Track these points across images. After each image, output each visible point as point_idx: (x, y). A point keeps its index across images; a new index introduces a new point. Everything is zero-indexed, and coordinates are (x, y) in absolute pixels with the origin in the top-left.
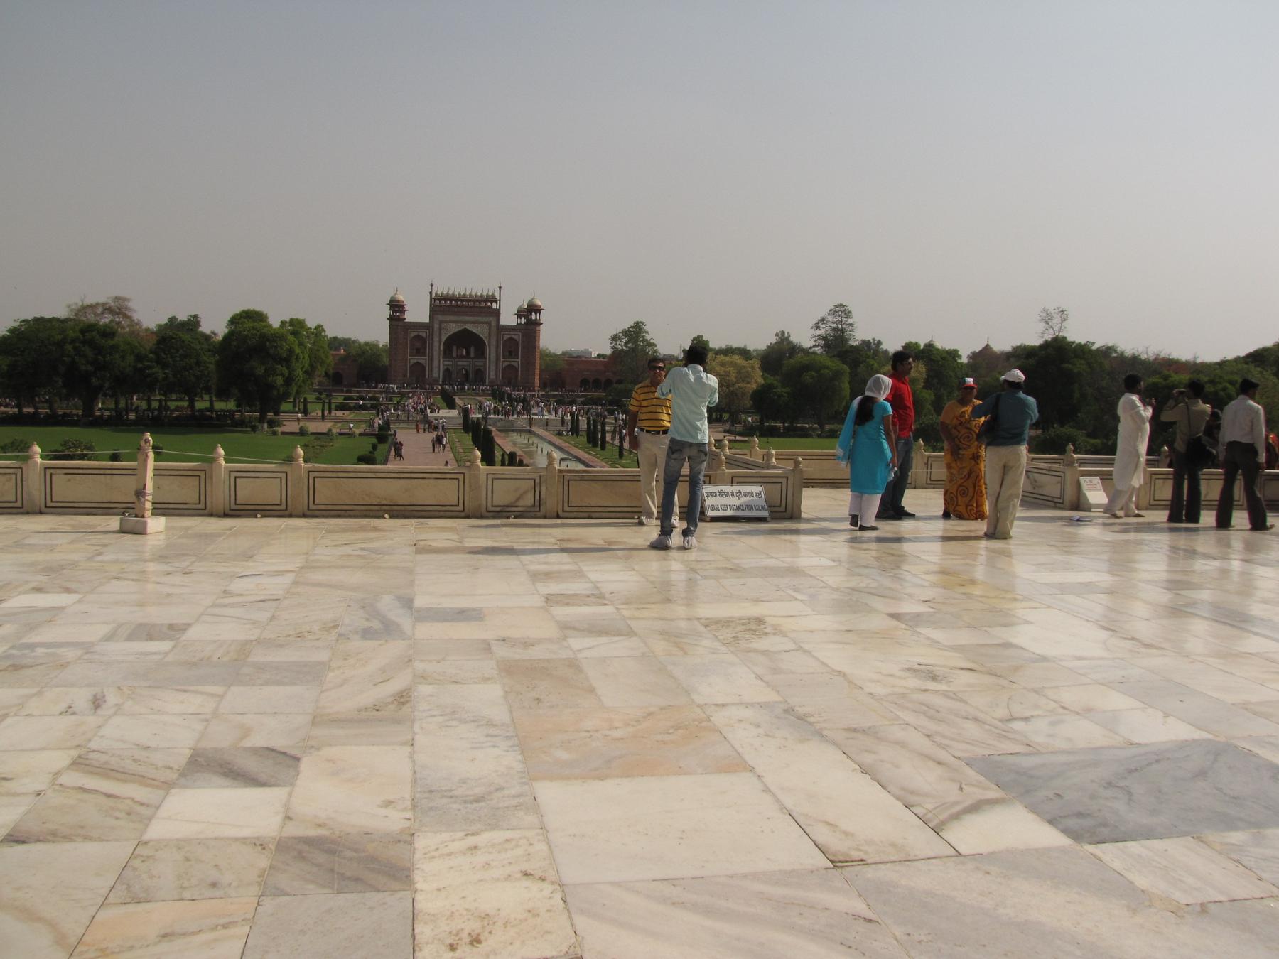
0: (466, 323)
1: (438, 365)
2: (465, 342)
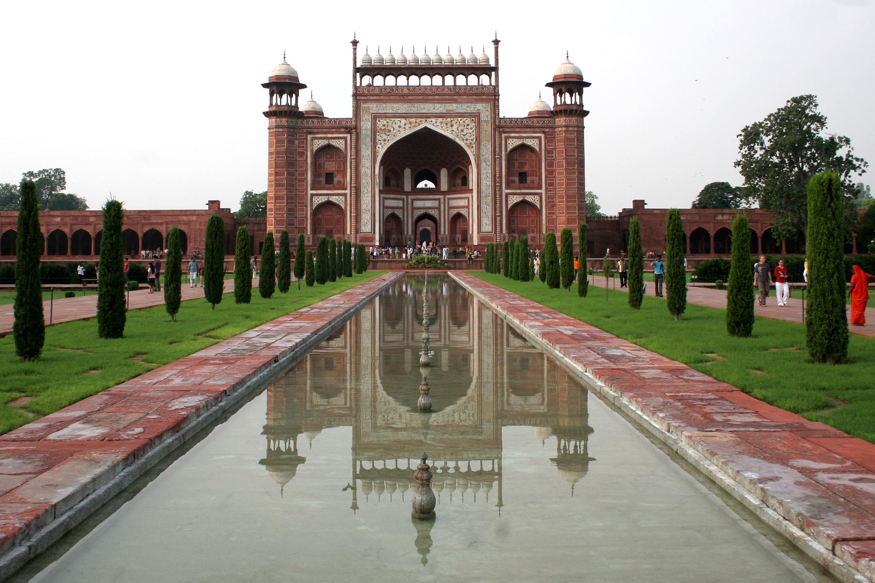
0: (427, 116)
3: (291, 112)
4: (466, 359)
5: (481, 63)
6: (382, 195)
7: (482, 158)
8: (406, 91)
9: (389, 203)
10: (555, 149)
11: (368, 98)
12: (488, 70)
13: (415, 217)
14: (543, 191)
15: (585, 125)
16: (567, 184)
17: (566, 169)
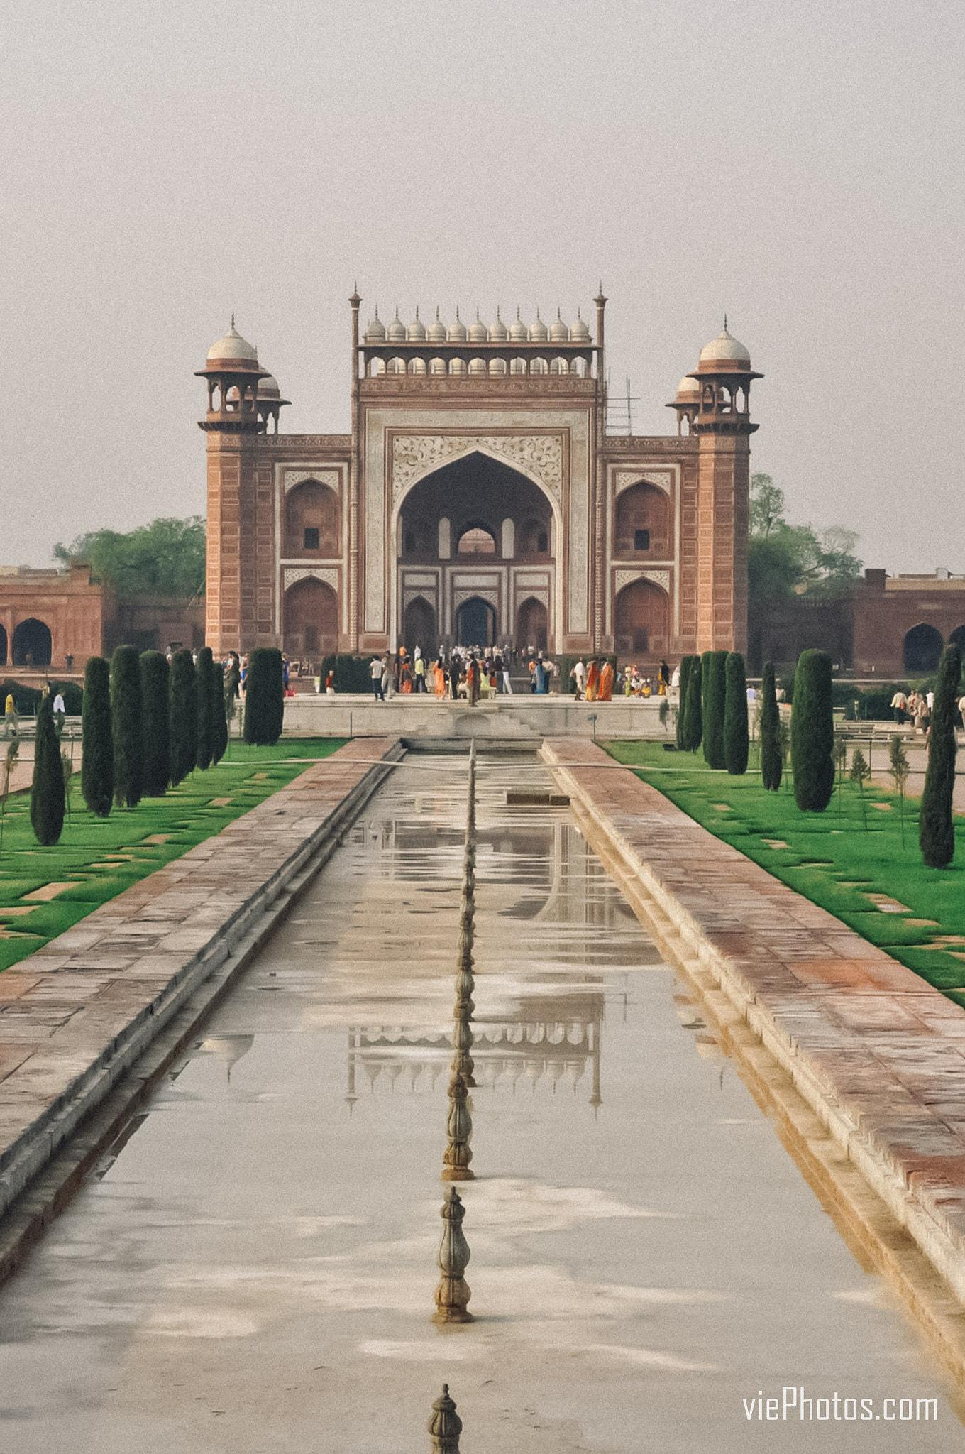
0: (478, 433)
2: (474, 498)
5: (575, 340)
6: (401, 567)
8: (443, 388)
9: (413, 580)
10: (697, 490)
13: (457, 604)
14: (675, 564)
16: (716, 552)
17: (715, 526)
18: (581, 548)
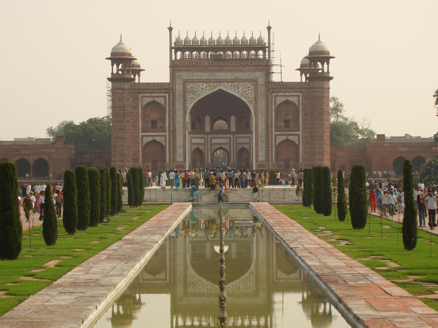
0: (221, 81)
1: (183, 144)
2: (220, 108)
3: (128, 79)
4: (249, 252)
6: (190, 136)
7: (259, 111)
8: (206, 64)
9: (195, 141)
11: (180, 68)
12: (263, 49)
13: (213, 150)
14: (300, 133)
15: (330, 86)
18: (262, 127)
